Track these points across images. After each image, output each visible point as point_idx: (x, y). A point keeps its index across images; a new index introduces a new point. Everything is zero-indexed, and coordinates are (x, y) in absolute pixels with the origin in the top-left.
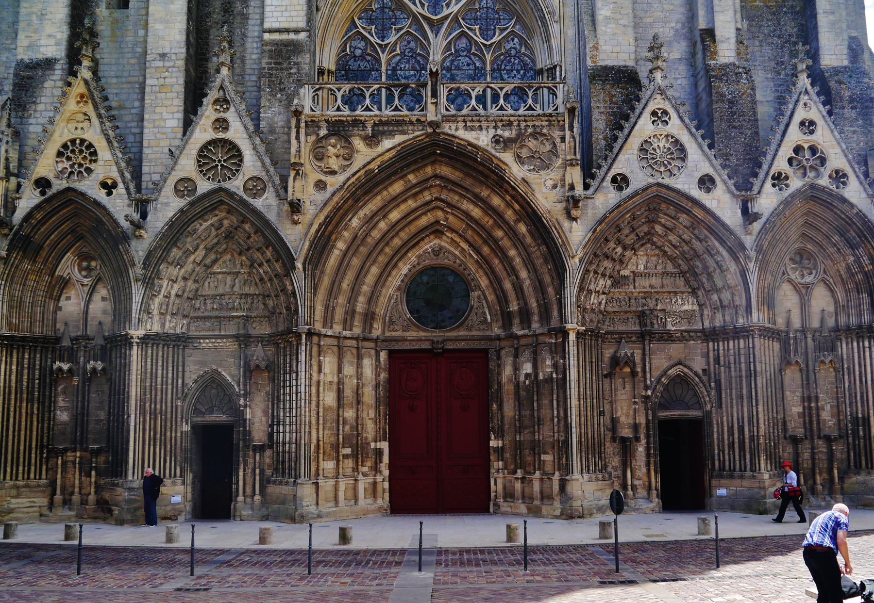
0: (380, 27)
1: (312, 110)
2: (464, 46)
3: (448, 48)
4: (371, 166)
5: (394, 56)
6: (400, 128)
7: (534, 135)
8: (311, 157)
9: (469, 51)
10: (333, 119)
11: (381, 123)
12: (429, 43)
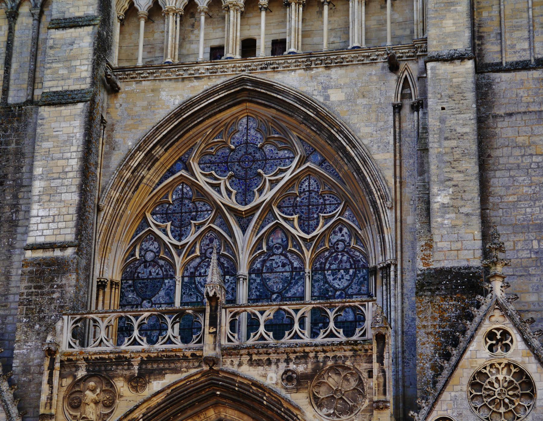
0: (177, 223)
1: (70, 346)
2: (279, 241)
3: (258, 245)
4: (135, 415)
5: (192, 259)
6: (173, 365)
7: (334, 369)
8: (66, 404)
9: (285, 247)
10: (93, 357)
11: (150, 360)
12: (235, 242)
